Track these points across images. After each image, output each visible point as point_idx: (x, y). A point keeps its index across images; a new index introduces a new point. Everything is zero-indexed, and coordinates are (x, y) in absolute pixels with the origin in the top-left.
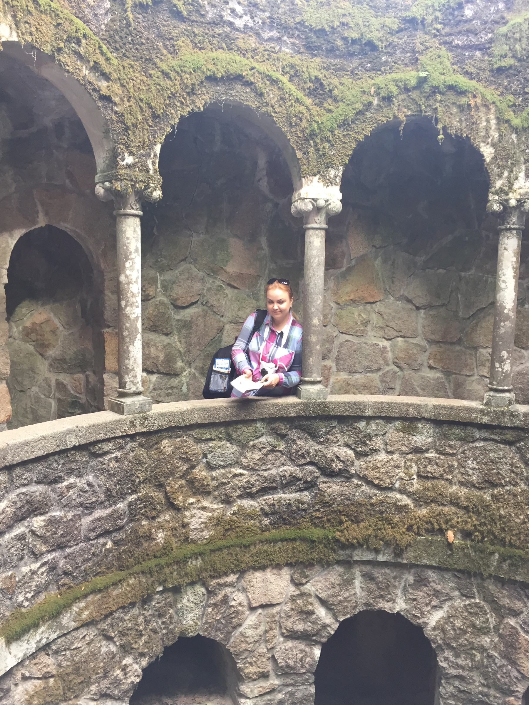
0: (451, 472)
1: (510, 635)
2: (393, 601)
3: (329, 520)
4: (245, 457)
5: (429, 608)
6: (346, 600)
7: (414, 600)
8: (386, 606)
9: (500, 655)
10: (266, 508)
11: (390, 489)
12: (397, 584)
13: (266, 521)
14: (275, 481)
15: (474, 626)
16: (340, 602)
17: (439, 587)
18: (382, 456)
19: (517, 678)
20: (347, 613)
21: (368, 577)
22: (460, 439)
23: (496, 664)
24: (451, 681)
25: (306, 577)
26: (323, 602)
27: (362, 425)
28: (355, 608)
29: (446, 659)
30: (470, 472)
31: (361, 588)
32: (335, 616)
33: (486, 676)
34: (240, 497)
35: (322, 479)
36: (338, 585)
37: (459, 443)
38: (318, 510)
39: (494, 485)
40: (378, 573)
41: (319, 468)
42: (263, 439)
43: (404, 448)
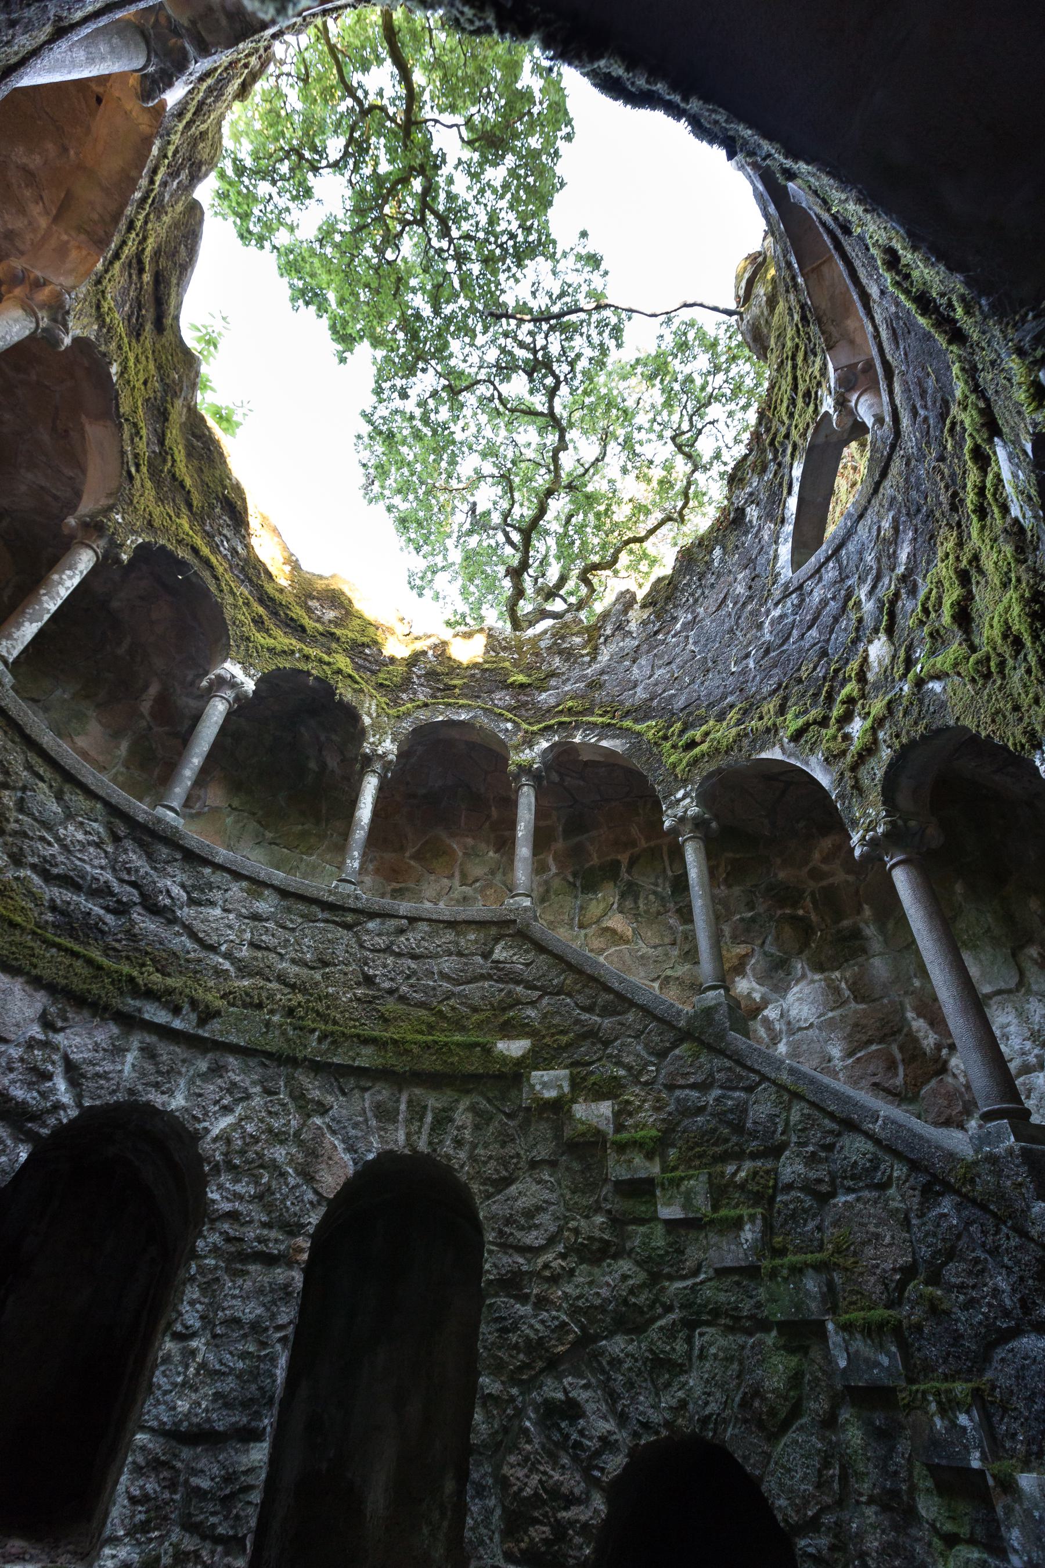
0: (285, 947)
1: (313, 1139)
2: (171, 1093)
3: (128, 958)
4: (66, 828)
5: (217, 1108)
6: (105, 1076)
7: (200, 1095)
8: (157, 1099)
9: (296, 1170)
10: (58, 901)
11: (213, 949)
12: (184, 1070)
13: (49, 917)
14: (83, 878)
15: (270, 1130)
16: (98, 1075)
17: (238, 1078)
18: (218, 912)
19: (311, 1203)
20: (100, 1097)
21: (149, 1053)
22: (302, 916)
23: (287, 1185)
24: (218, 1225)
25: (65, 1019)
26: (71, 1069)
27: (207, 871)
28: (114, 1092)
29: (220, 1187)
30: (305, 949)
31: (133, 1065)
32: (78, 1098)
33: (268, 1208)
34: (33, 867)
35: (139, 909)
36: (104, 1050)
37: (300, 920)
38: (119, 941)
39: (326, 964)
40: (166, 1051)
41: (142, 894)
42: (95, 825)
43: (243, 910)
